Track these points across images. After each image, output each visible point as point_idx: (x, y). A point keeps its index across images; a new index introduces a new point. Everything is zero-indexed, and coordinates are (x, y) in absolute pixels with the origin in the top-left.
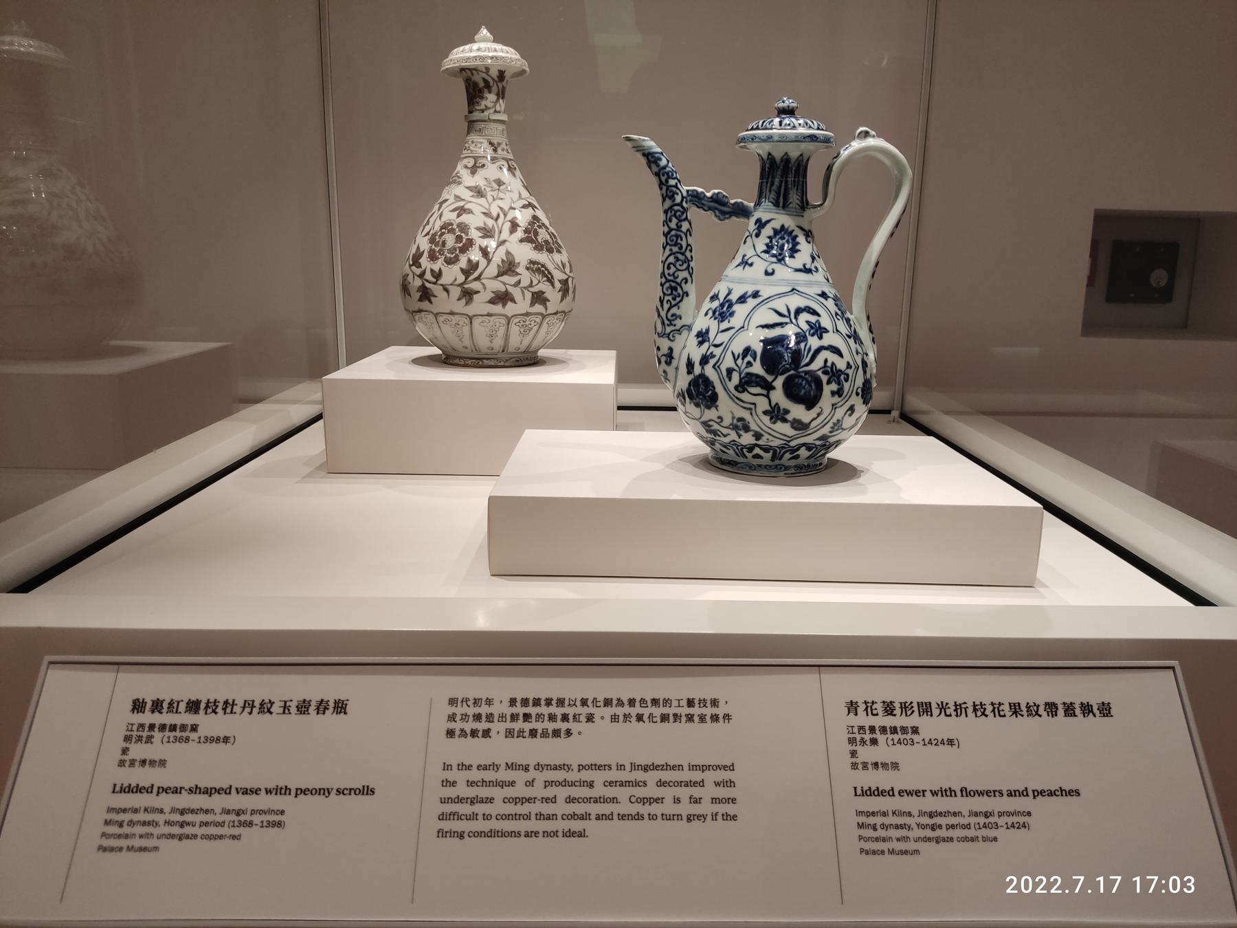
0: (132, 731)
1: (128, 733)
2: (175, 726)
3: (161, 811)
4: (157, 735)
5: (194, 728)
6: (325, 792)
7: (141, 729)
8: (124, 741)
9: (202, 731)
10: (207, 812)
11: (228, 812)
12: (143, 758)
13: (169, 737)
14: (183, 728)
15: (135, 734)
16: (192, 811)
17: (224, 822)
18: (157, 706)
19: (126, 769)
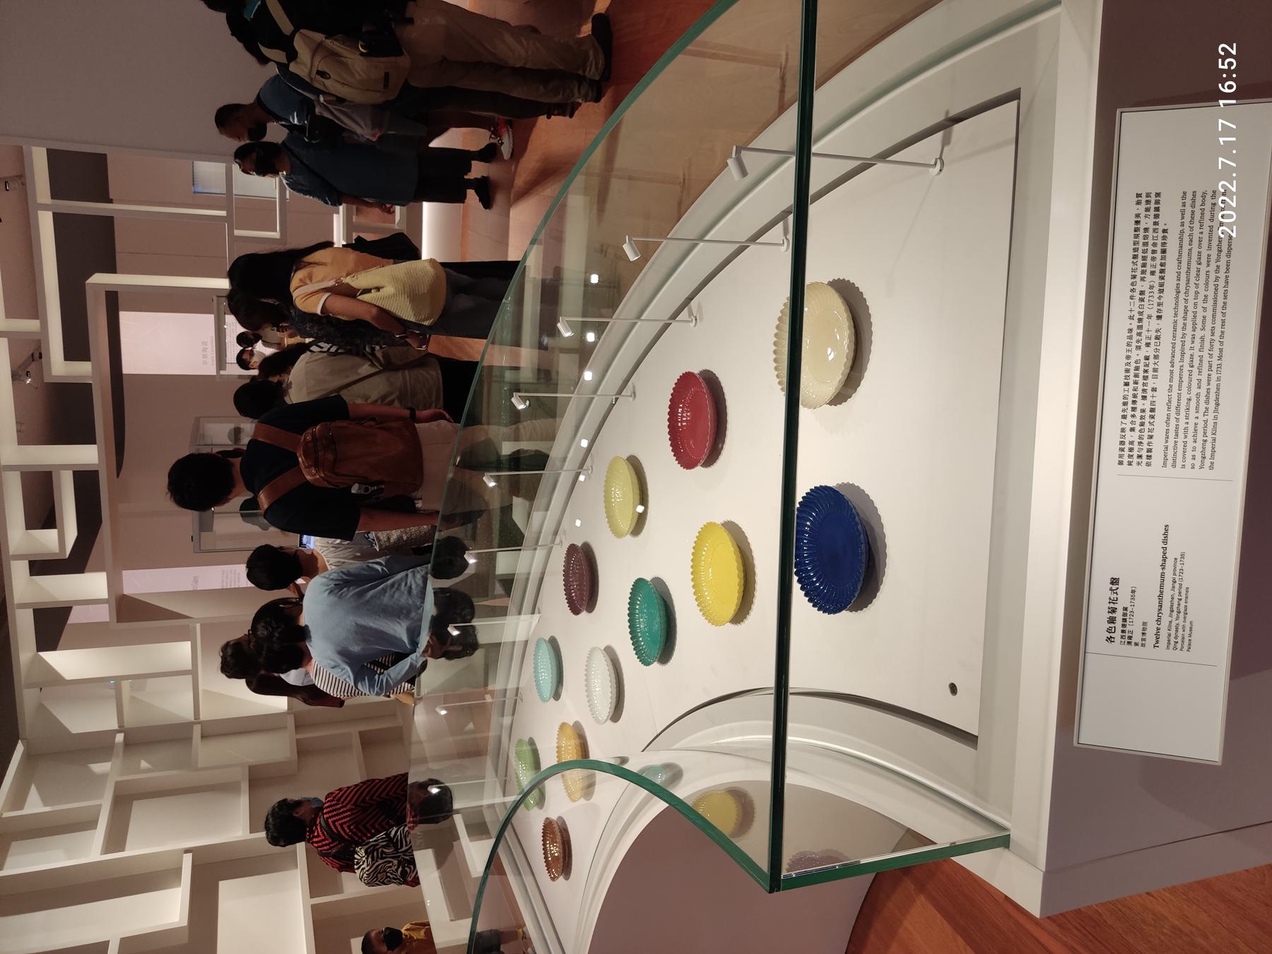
1: (1126, 643)
2: (1123, 619)
4: (1128, 628)
6: (1165, 541)
9: (1127, 605)
11: (1174, 587)
14: (1125, 615)
15: (1127, 640)
16: (1172, 606)
19: (1147, 643)
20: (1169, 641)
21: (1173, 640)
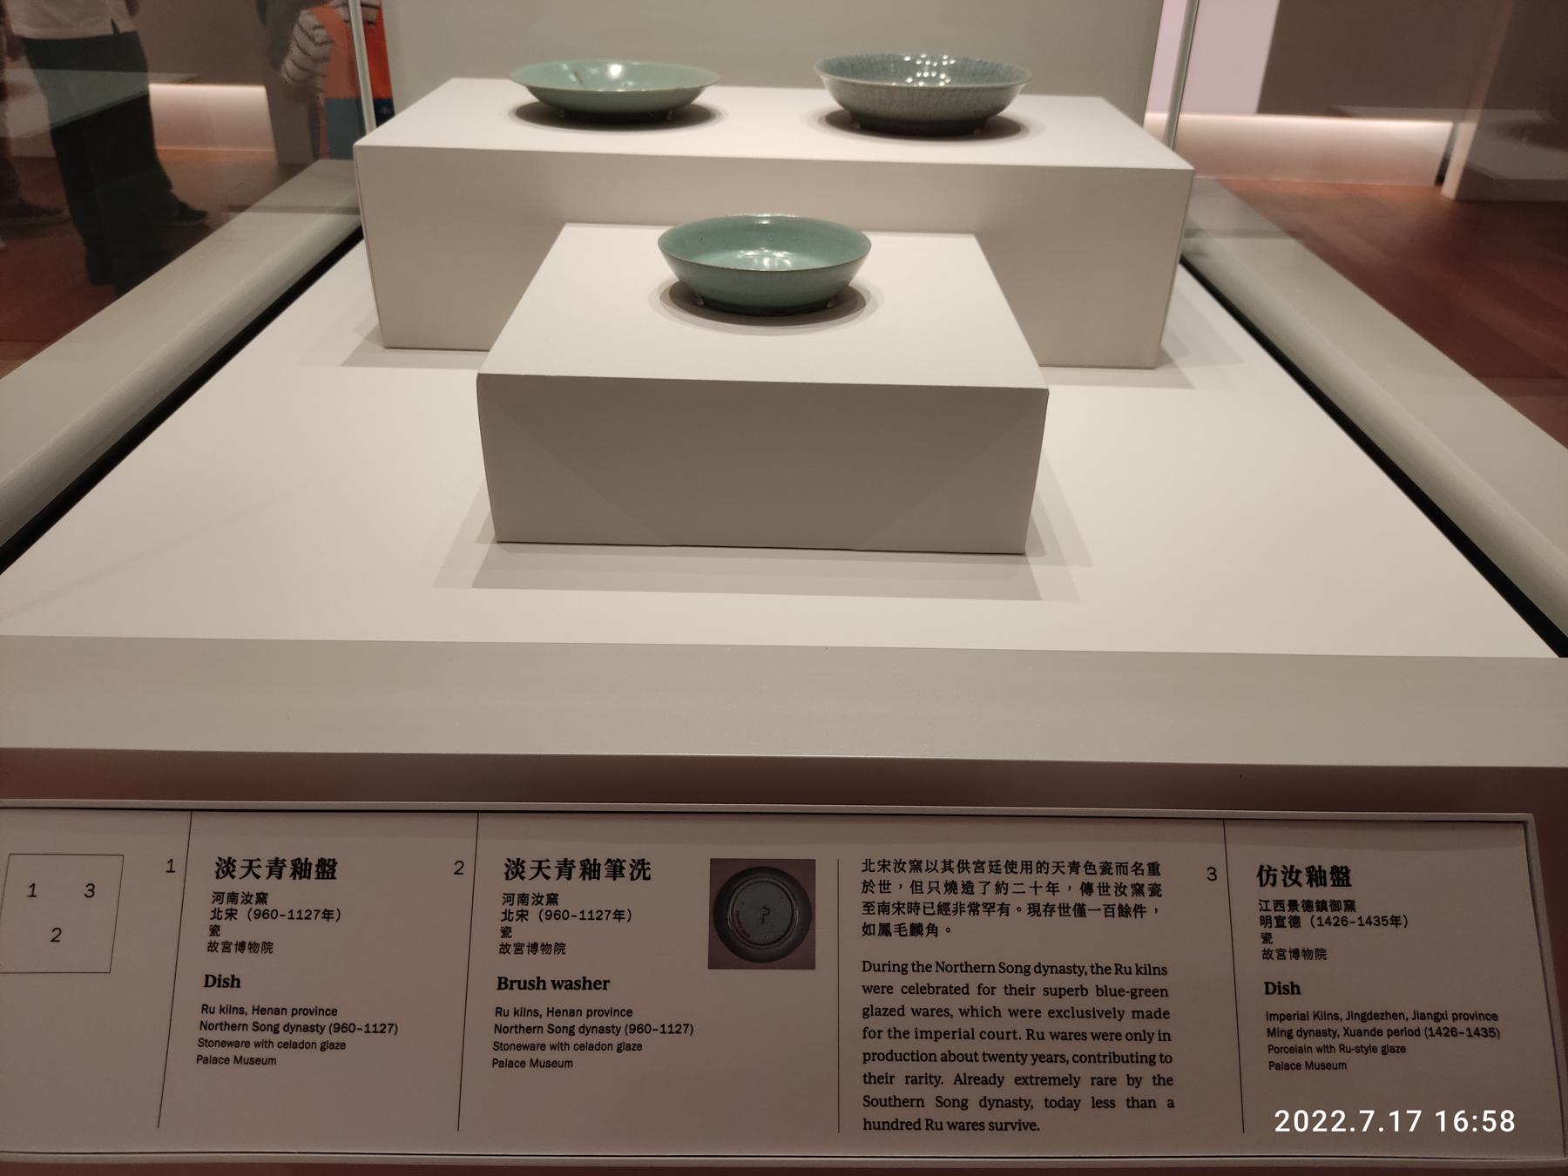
0: (1267, 910)
1: (1265, 914)
2: (1324, 902)
3: (1336, 1017)
4: (1305, 917)
5: (1350, 906)
7: (1279, 908)
8: (1261, 924)
9: (1363, 910)
10: (1395, 1016)
12: (1293, 948)
13: (1320, 918)
14: (1335, 905)
15: (1273, 914)
16: (1376, 1016)
17: (1418, 1030)
18: (1291, 874)
20: (1289, 1017)
21: (1295, 1025)
